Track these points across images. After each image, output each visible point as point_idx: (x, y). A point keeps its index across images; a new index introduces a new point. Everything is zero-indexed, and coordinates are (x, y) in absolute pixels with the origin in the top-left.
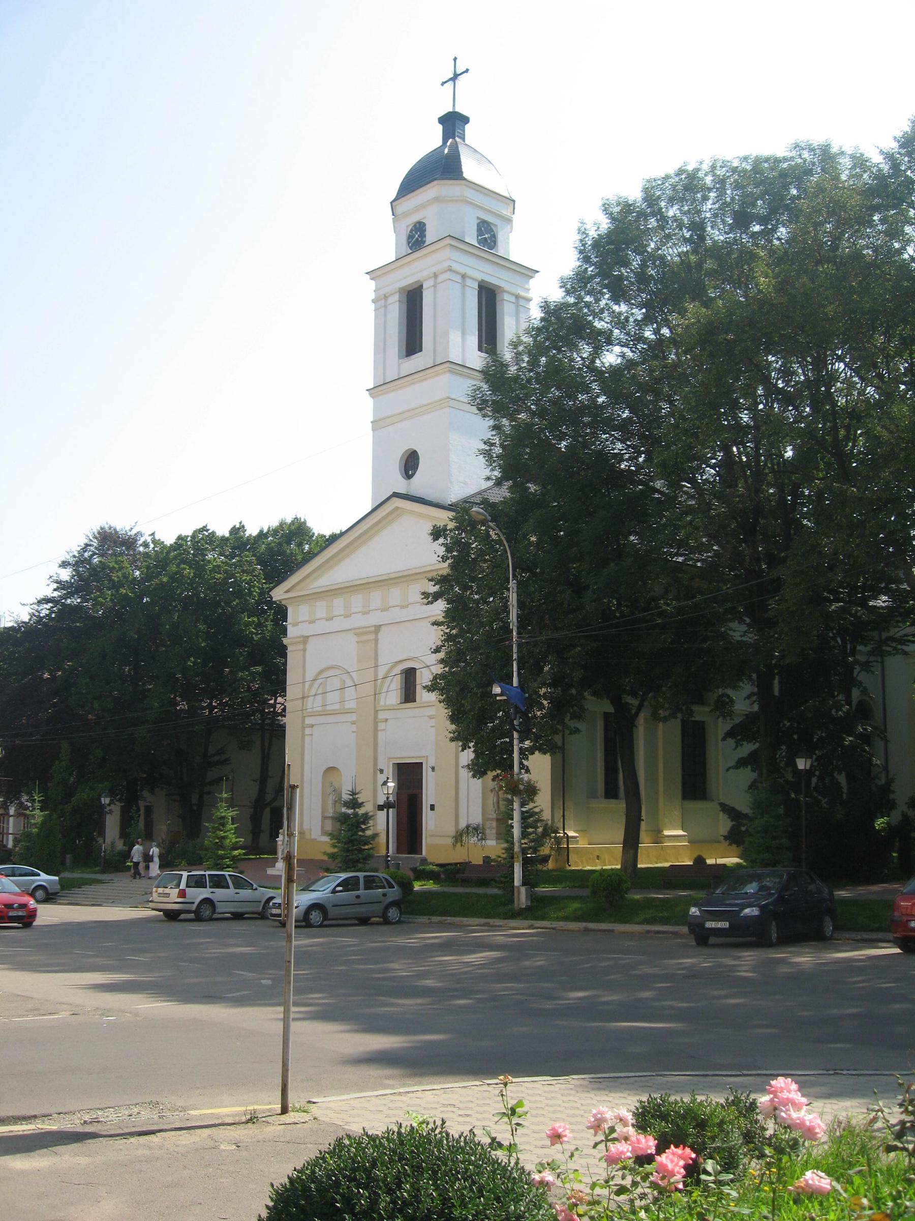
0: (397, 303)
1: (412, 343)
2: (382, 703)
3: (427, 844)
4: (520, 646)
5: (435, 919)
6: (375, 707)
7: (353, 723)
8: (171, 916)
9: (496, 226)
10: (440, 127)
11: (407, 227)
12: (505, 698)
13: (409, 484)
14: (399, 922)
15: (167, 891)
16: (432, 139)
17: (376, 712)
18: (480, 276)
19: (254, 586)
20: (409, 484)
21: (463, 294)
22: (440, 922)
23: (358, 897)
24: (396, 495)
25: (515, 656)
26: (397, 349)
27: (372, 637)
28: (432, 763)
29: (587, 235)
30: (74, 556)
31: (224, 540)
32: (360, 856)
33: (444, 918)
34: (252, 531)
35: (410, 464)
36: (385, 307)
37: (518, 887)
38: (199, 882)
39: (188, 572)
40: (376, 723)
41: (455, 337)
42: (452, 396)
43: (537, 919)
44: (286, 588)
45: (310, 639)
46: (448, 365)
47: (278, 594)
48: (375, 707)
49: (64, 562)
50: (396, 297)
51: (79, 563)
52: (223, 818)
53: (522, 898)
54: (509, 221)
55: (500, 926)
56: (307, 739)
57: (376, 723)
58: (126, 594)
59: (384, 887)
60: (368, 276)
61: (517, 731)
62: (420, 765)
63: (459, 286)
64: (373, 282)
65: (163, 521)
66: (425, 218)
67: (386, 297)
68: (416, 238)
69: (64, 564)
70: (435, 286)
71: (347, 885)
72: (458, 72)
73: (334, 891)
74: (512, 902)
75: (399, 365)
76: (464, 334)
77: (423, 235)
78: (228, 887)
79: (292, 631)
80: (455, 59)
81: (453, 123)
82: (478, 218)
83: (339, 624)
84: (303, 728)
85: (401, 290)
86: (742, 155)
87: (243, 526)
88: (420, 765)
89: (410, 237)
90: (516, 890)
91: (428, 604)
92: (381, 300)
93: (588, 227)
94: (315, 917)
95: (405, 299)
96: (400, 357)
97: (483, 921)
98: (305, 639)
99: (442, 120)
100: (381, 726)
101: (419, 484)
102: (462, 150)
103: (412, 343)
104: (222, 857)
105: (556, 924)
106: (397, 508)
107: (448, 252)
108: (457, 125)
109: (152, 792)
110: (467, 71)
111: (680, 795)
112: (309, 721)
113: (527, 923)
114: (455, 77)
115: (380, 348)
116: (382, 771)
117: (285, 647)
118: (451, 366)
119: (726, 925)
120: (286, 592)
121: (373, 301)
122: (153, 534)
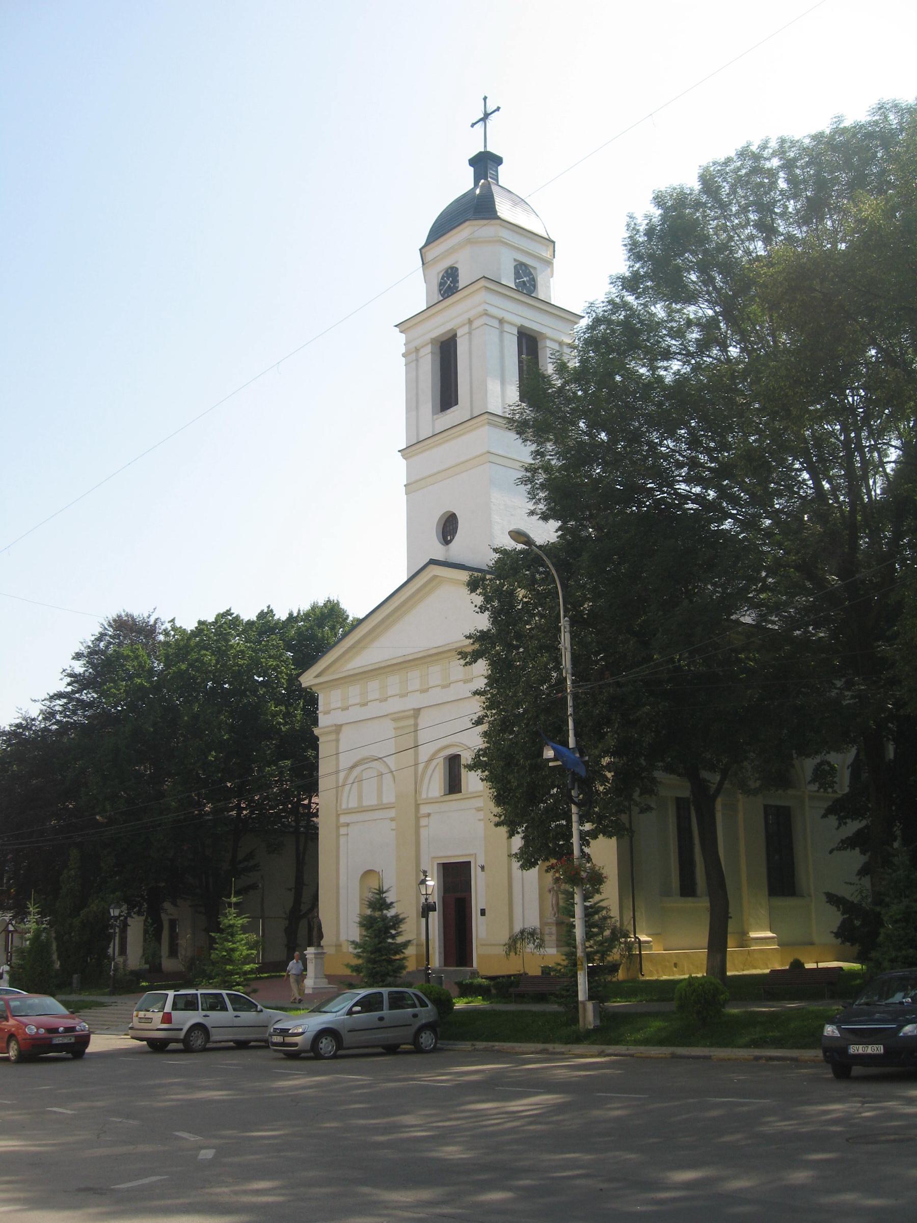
0: (430, 356)
1: (447, 396)
2: (424, 796)
3: (478, 956)
4: (575, 697)
5: (481, 1045)
6: (416, 800)
7: (392, 819)
8: (158, 1046)
9: (535, 268)
10: (472, 169)
11: (438, 274)
12: (559, 763)
13: (447, 551)
14: (434, 1050)
15: (149, 1015)
16: (464, 181)
17: (417, 806)
18: (519, 321)
19: (281, 672)
20: (447, 551)
21: (502, 340)
22: (485, 1050)
23: (381, 1019)
24: (433, 562)
25: (570, 711)
27: (411, 722)
28: (481, 861)
29: (638, 231)
30: (89, 647)
31: (250, 623)
32: (390, 967)
33: (491, 1044)
34: (281, 615)
35: (449, 527)
36: (417, 360)
37: (583, 1003)
38: (190, 1004)
39: (208, 657)
40: (417, 819)
41: (494, 386)
42: (492, 451)
43: (609, 1043)
44: (315, 674)
45: (344, 729)
46: (486, 416)
47: (307, 679)
48: (416, 800)
49: (77, 654)
50: (429, 349)
51: (92, 655)
52: (231, 926)
53: (589, 1016)
54: (549, 263)
55: (563, 1053)
56: (342, 840)
57: (417, 819)
58: (141, 684)
59: (414, 1006)
60: (397, 329)
61: (575, 803)
62: (469, 862)
63: (497, 332)
64: (403, 335)
65: (183, 604)
66: (457, 262)
67: (417, 350)
68: (448, 285)
69: (78, 656)
70: (470, 333)
71: (368, 1004)
72: (489, 111)
73: (350, 1013)
74: (575, 1020)
75: (433, 421)
76: (503, 383)
77: (455, 280)
78: (227, 1010)
79: (323, 720)
80: (485, 99)
81: (485, 164)
82: (515, 260)
83: (374, 709)
84: (338, 827)
85: (433, 341)
86: (813, 132)
87: (272, 611)
88: (469, 862)
89: (441, 284)
90: (580, 1006)
91: (466, 665)
92: (412, 354)
93: (639, 221)
94: (326, 1045)
95: (438, 351)
96: (434, 413)
97: (541, 1046)
98: (338, 728)
99: (473, 162)
100: (423, 822)
101: (459, 550)
102: (495, 189)
103: (447, 396)
104: (231, 973)
105: (633, 1050)
106: (435, 577)
107: (483, 296)
108: (489, 166)
109: (175, 904)
110: (498, 109)
111: (766, 891)
112: (343, 819)
113: (596, 1048)
114: (486, 116)
115: (413, 405)
117: (317, 739)
118: (491, 417)
119: (879, 1049)
120: (317, 676)
121: (404, 355)
122: (173, 621)
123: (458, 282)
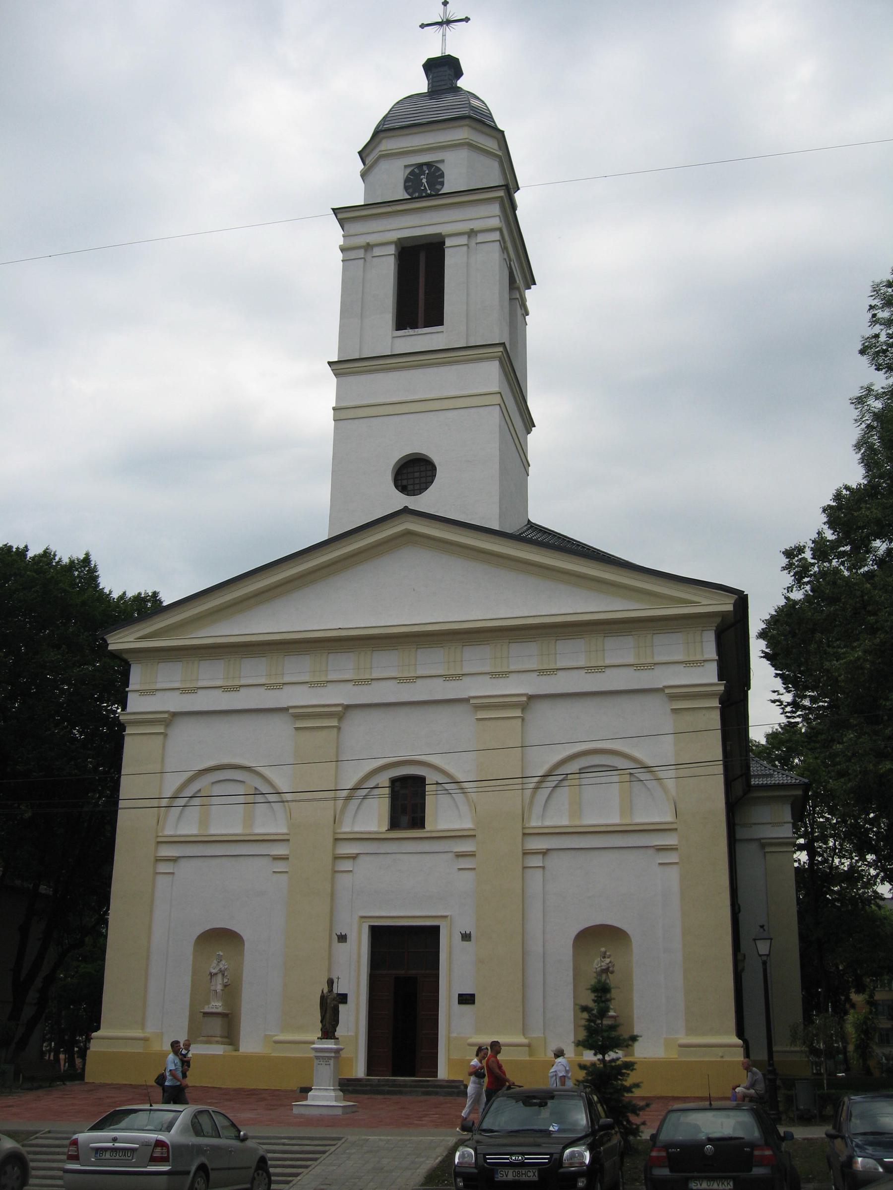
26: (391, 315)
50: (392, 250)
56: (161, 881)
62: (434, 931)
68: (424, 184)
79: (136, 703)
88: (434, 931)
106: (408, 533)
112: (165, 852)
116: (342, 938)
123: (442, 184)
